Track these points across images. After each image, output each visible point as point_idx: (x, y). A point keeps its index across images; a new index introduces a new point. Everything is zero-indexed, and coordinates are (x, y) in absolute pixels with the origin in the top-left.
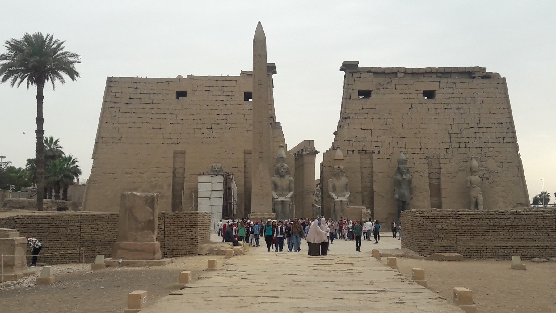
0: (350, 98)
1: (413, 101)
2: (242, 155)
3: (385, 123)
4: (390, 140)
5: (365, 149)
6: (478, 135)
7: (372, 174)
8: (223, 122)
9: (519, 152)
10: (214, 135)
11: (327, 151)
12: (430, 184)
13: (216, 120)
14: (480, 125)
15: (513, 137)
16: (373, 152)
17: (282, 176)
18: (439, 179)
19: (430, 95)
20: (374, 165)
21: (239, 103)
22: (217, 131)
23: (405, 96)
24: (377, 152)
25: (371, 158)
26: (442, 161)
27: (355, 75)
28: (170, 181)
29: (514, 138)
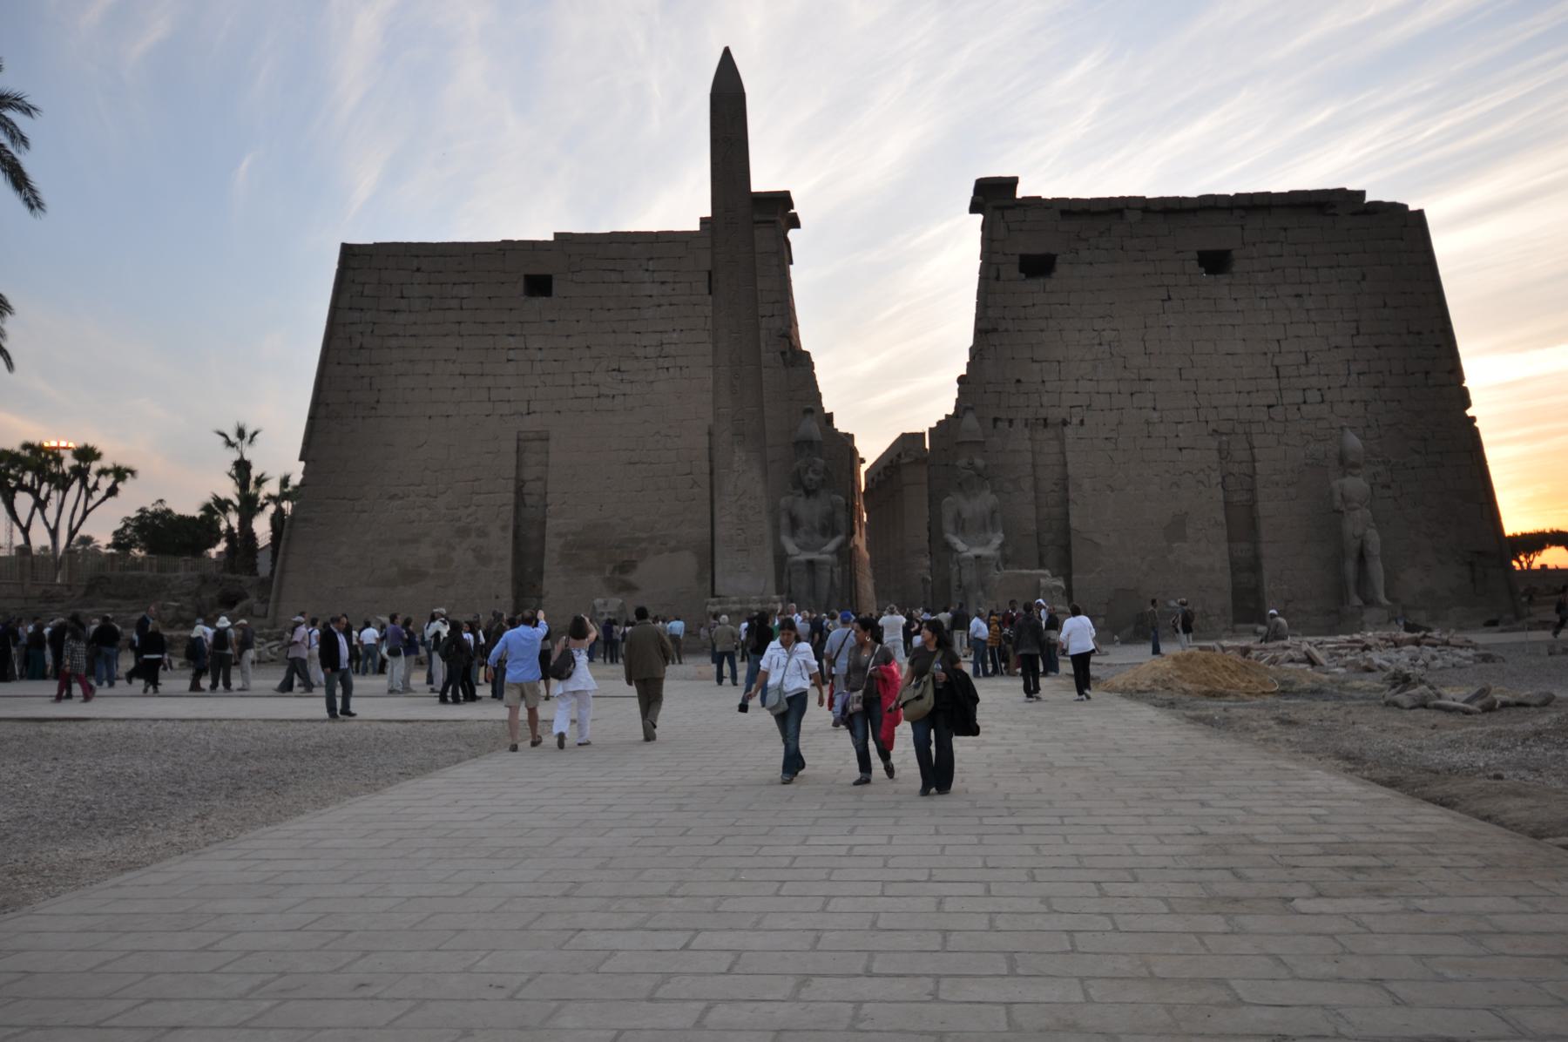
0: (998, 278)
3: (1096, 341)
5: (1042, 413)
7: (1064, 482)
8: (651, 352)
9: (1469, 412)
11: (939, 423)
12: (1227, 504)
16: (1065, 423)
17: (809, 493)
18: (1252, 490)
19: (1215, 262)
20: (1070, 456)
24: (1075, 421)
25: (1061, 440)
28: (508, 512)
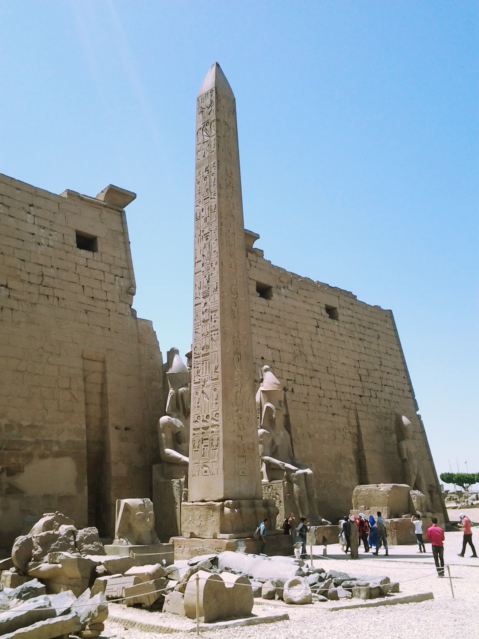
1: (317, 317)
2: (78, 363)
4: (301, 371)
6: (384, 382)
8: (34, 279)
9: (418, 413)
10: (13, 303)
13: (19, 273)
14: (383, 368)
15: (410, 391)
19: (331, 312)
21: (67, 248)
22: (19, 297)
23: (308, 307)
24: (290, 389)
26: (361, 415)
27: (249, 254)
29: (411, 391)
